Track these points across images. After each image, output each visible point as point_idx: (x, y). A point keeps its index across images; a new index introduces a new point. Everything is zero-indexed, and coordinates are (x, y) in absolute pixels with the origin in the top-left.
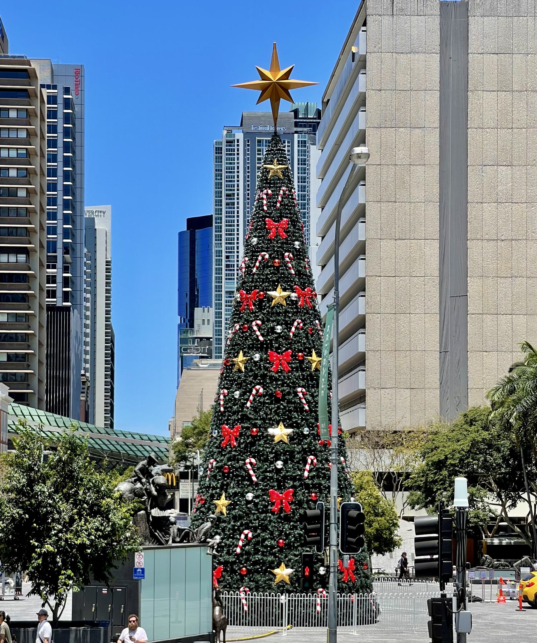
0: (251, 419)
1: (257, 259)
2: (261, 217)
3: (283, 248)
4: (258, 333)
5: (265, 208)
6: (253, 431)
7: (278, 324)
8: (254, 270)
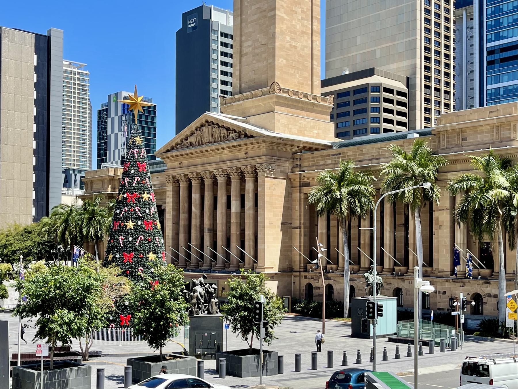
4: (139, 213)
5: (136, 157)
8: (134, 184)
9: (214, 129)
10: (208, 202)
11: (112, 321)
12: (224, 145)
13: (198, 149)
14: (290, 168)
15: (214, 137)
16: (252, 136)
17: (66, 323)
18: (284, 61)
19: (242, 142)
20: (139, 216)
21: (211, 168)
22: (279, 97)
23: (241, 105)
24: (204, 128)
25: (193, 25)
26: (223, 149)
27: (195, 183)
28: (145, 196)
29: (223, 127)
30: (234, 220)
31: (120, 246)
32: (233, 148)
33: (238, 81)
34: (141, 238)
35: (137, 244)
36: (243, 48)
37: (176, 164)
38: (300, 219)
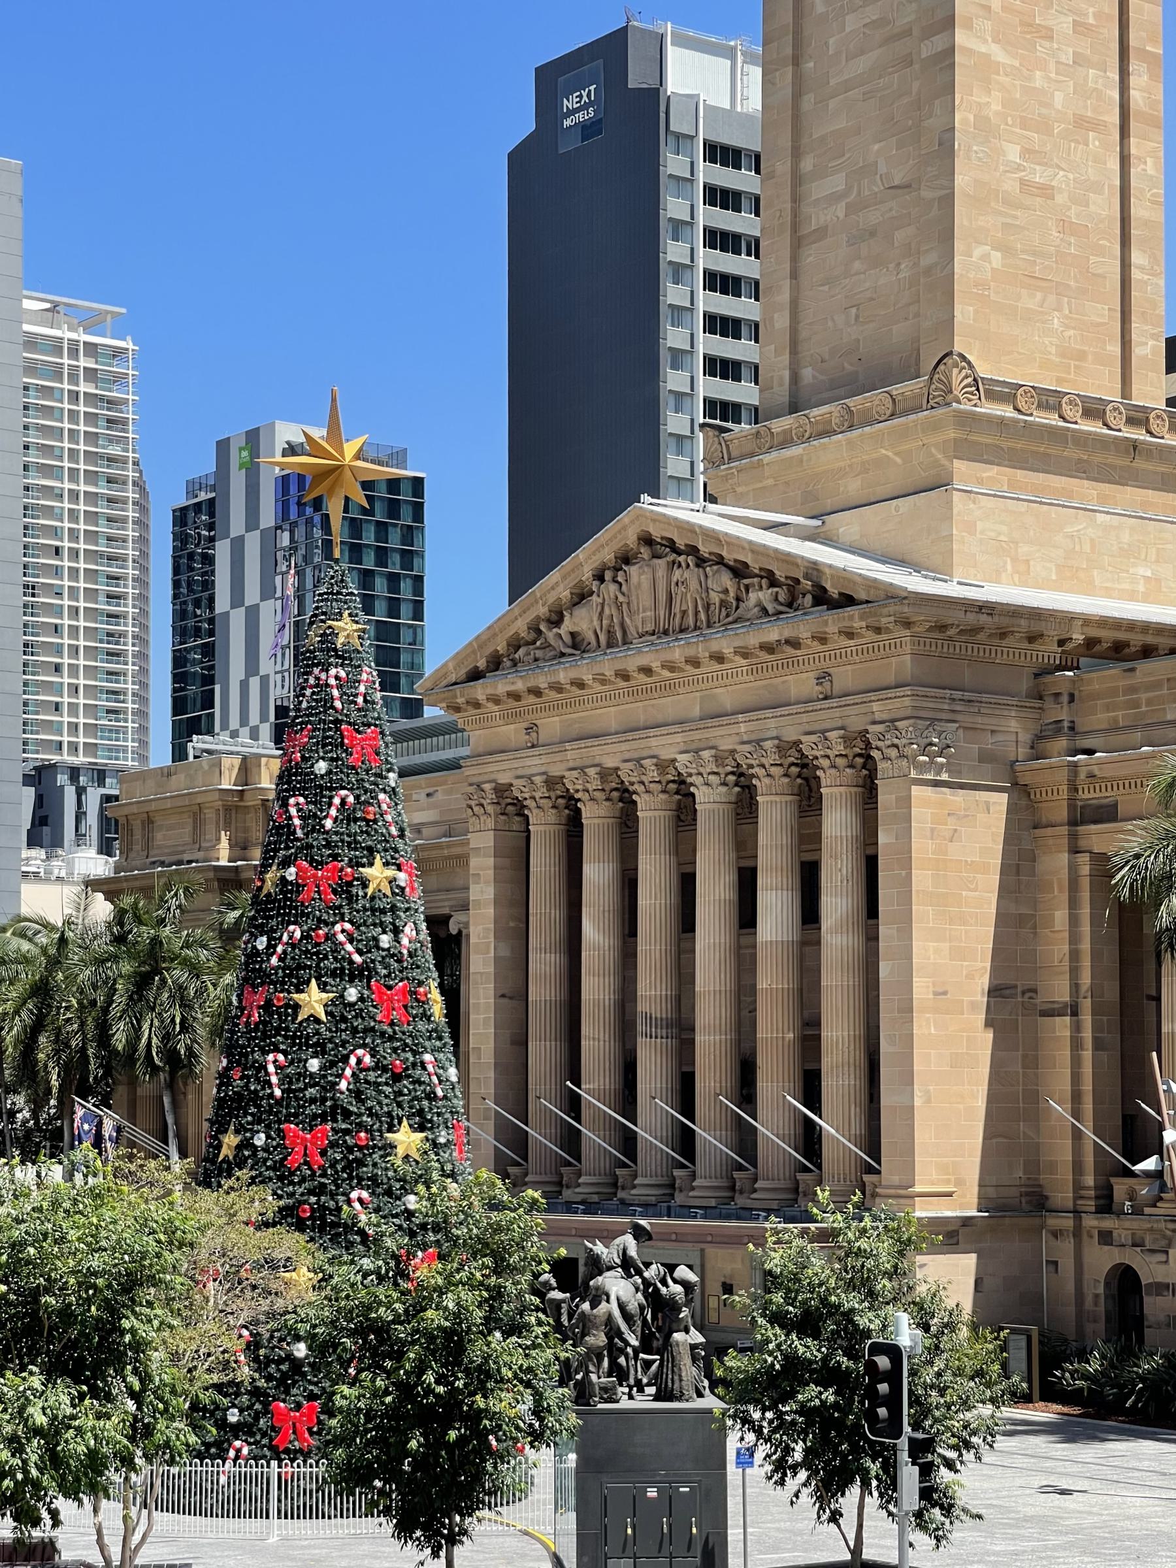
0: (351, 1113)
1: (330, 804)
2: (331, 722)
3: (377, 785)
4: (349, 947)
5: (338, 704)
6: (360, 1139)
7: (384, 932)
8: (328, 824)
9: (677, 574)
10: (654, 898)
11: (236, 1430)
12: (724, 643)
13: (607, 665)
14: (1025, 737)
15: (676, 609)
16: (848, 600)
17: (38, 1431)
18: (996, 256)
19: (803, 625)
20: (351, 962)
21: (667, 746)
23: (800, 460)
24: (633, 570)
26: (719, 658)
27: (596, 817)
28: (377, 873)
29: (720, 561)
30: (772, 980)
31: (271, 1095)
32: (764, 656)
33: (786, 358)
34: (359, 1061)
35: (343, 1085)
36: (806, 209)
37: (512, 732)
38: (1074, 971)
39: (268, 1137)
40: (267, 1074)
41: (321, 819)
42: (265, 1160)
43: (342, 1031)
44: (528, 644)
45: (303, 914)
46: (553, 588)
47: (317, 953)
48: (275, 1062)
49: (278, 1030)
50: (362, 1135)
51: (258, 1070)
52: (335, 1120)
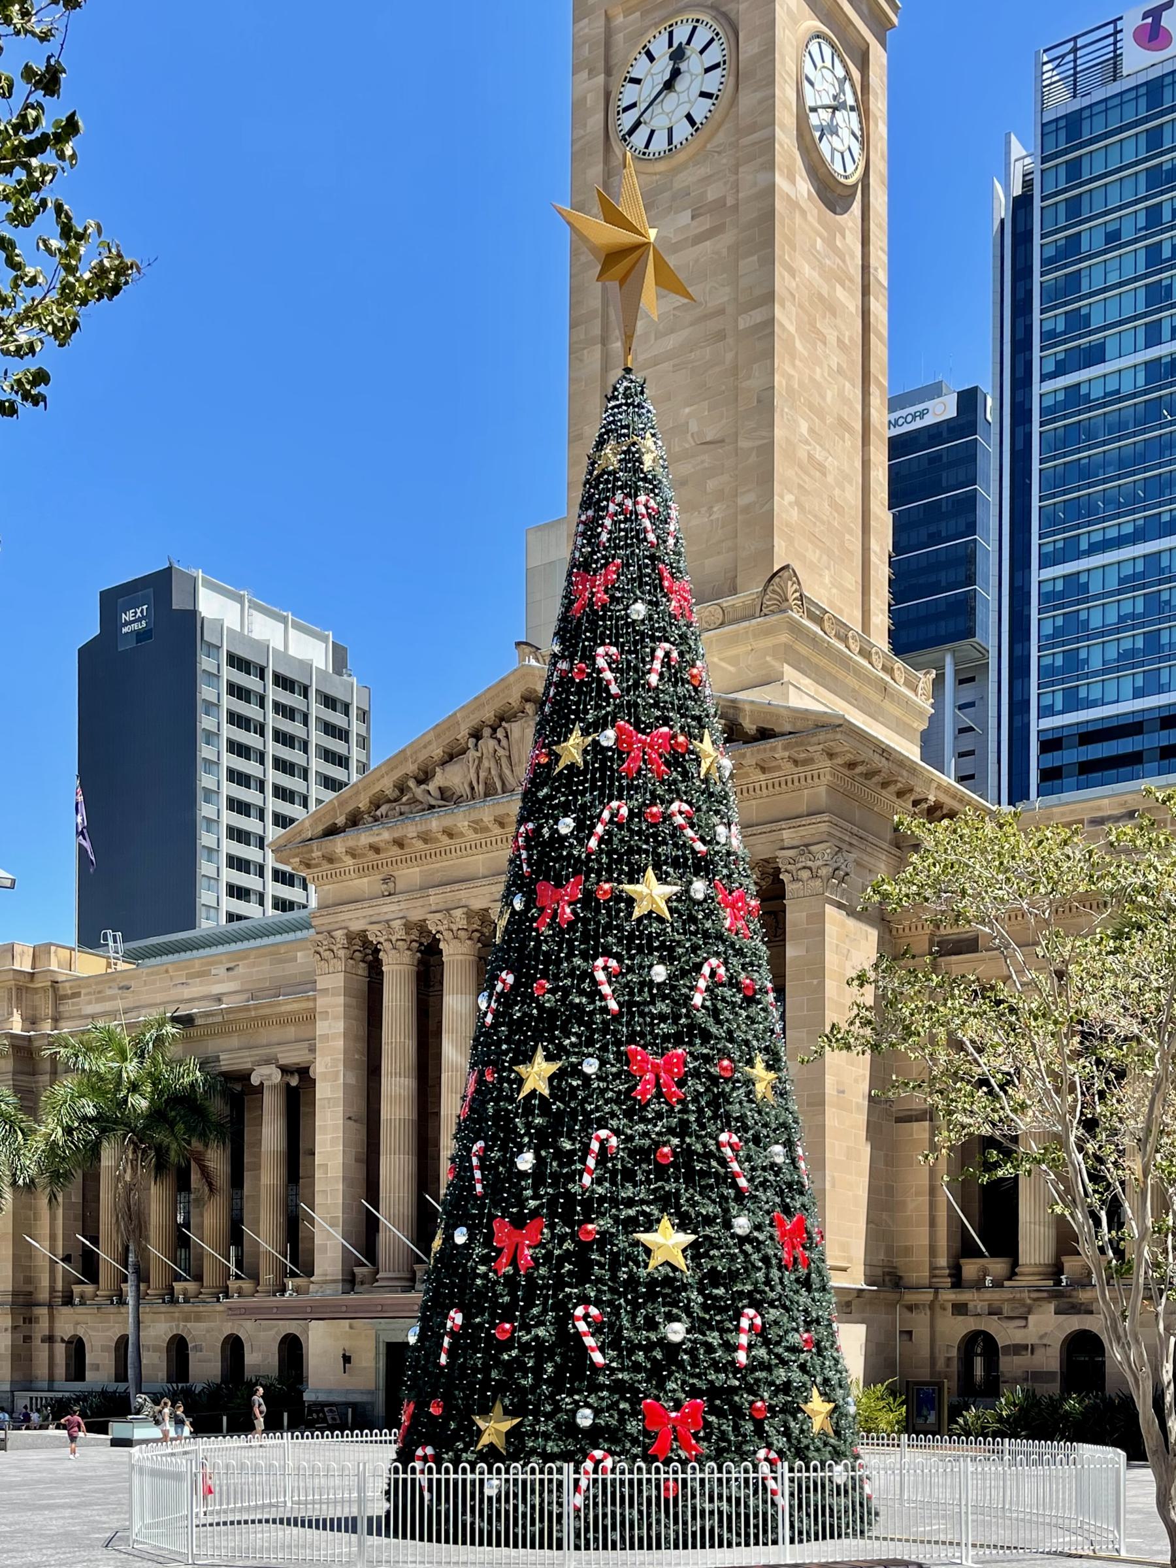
20: (694, 851)
22: (796, 629)
25: (135, 626)
31: (605, 1010)
35: (698, 999)
39: (603, 1063)
40: (595, 983)
41: (644, 674)
42: (603, 1092)
43: (691, 933)
44: (389, 801)
45: (630, 787)
46: (425, 747)
47: (655, 835)
48: (605, 968)
49: (608, 927)
50: (726, 1063)
51: (582, 978)
52: (691, 1043)
